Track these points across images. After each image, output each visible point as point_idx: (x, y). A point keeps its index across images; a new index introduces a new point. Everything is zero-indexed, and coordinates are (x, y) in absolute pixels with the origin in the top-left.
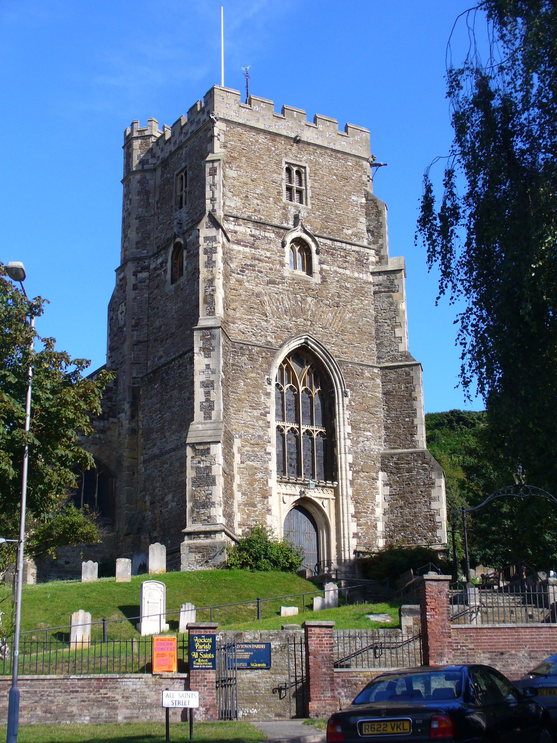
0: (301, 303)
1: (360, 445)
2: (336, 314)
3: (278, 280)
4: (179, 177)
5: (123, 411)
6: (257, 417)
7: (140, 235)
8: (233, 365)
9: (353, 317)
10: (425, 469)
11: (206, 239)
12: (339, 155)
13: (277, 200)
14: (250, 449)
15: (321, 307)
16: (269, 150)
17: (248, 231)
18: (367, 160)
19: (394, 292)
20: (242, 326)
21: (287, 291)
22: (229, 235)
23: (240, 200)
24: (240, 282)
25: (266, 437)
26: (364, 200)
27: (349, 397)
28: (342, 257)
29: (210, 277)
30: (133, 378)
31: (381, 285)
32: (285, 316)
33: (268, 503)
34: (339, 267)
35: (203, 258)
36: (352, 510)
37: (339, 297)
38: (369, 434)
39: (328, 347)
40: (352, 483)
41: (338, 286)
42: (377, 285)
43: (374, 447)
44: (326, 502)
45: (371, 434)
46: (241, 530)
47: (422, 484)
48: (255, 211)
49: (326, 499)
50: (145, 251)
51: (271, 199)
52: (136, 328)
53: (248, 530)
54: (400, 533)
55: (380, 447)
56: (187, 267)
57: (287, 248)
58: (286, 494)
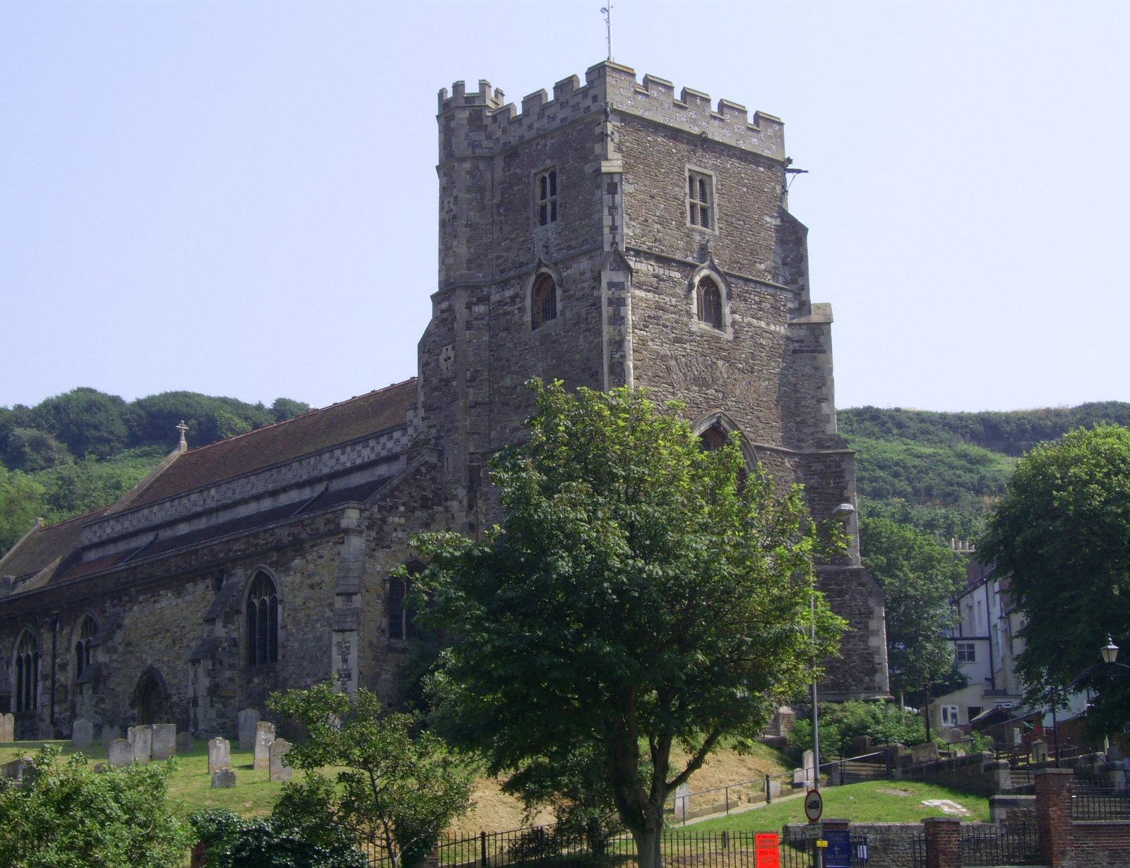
4: (539, 177)
5: (455, 497)
7: (472, 250)
9: (770, 387)
10: (861, 594)
11: (611, 285)
13: (681, 225)
16: (670, 154)
17: (651, 268)
19: (820, 352)
23: (638, 226)
26: (778, 222)
28: (756, 303)
29: (618, 338)
30: (470, 453)
35: (606, 310)
42: (797, 341)
48: (656, 241)
50: (481, 275)
51: (674, 223)
52: (473, 384)
56: (563, 313)
57: (694, 294)
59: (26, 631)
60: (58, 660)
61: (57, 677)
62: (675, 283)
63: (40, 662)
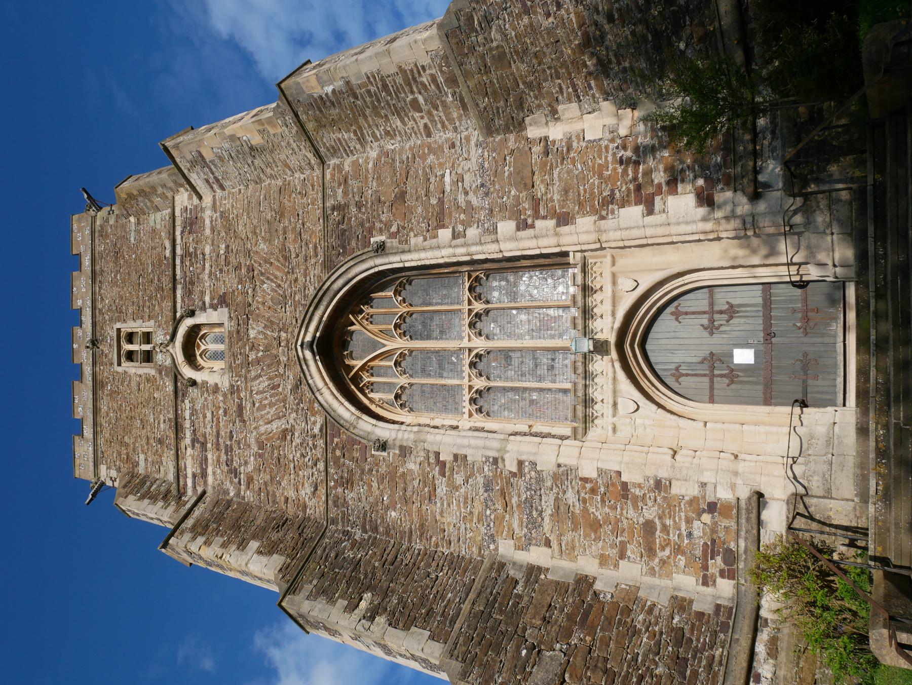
0: (258, 351)
1: (475, 201)
2: (262, 274)
3: (236, 400)
6: (448, 485)
8: (364, 531)
9: (263, 234)
12: (98, 268)
14: (516, 516)
15: (258, 309)
16: (112, 393)
17: (189, 451)
18: (94, 218)
20: (308, 489)
21: (246, 378)
22: (200, 490)
23: (165, 455)
24: (250, 480)
25: (486, 469)
26: (132, 219)
27: (383, 238)
31: (207, 181)
32: (280, 389)
33: (640, 486)
34: (204, 269)
36: (634, 212)
37: (238, 268)
38: (447, 179)
39: (311, 291)
40: (564, 219)
41: (225, 269)
42: (212, 188)
43: (474, 160)
44: (625, 284)
45: (448, 171)
46: (719, 580)
47: (526, 20)
49: (614, 283)
53: (719, 559)
54: (683, 53)
55: (473, 143)
58: (615, 405)
62: (194, 412)
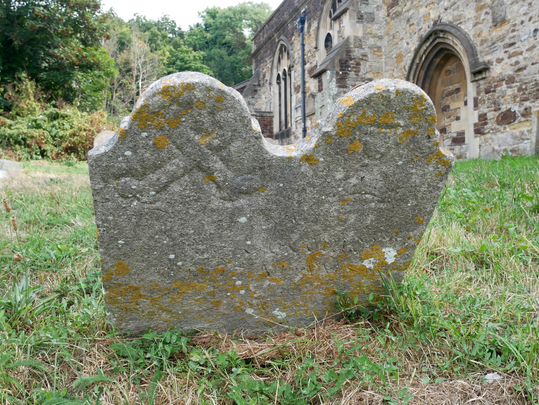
59: (282, 45)
60: (307, 66)
61: (307, 85)
63: (293, 72)
